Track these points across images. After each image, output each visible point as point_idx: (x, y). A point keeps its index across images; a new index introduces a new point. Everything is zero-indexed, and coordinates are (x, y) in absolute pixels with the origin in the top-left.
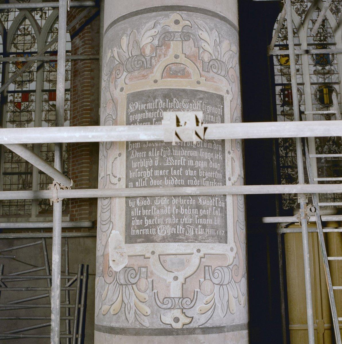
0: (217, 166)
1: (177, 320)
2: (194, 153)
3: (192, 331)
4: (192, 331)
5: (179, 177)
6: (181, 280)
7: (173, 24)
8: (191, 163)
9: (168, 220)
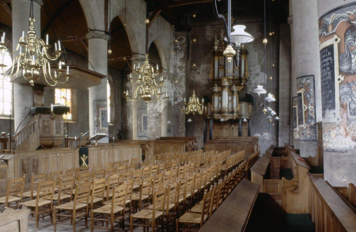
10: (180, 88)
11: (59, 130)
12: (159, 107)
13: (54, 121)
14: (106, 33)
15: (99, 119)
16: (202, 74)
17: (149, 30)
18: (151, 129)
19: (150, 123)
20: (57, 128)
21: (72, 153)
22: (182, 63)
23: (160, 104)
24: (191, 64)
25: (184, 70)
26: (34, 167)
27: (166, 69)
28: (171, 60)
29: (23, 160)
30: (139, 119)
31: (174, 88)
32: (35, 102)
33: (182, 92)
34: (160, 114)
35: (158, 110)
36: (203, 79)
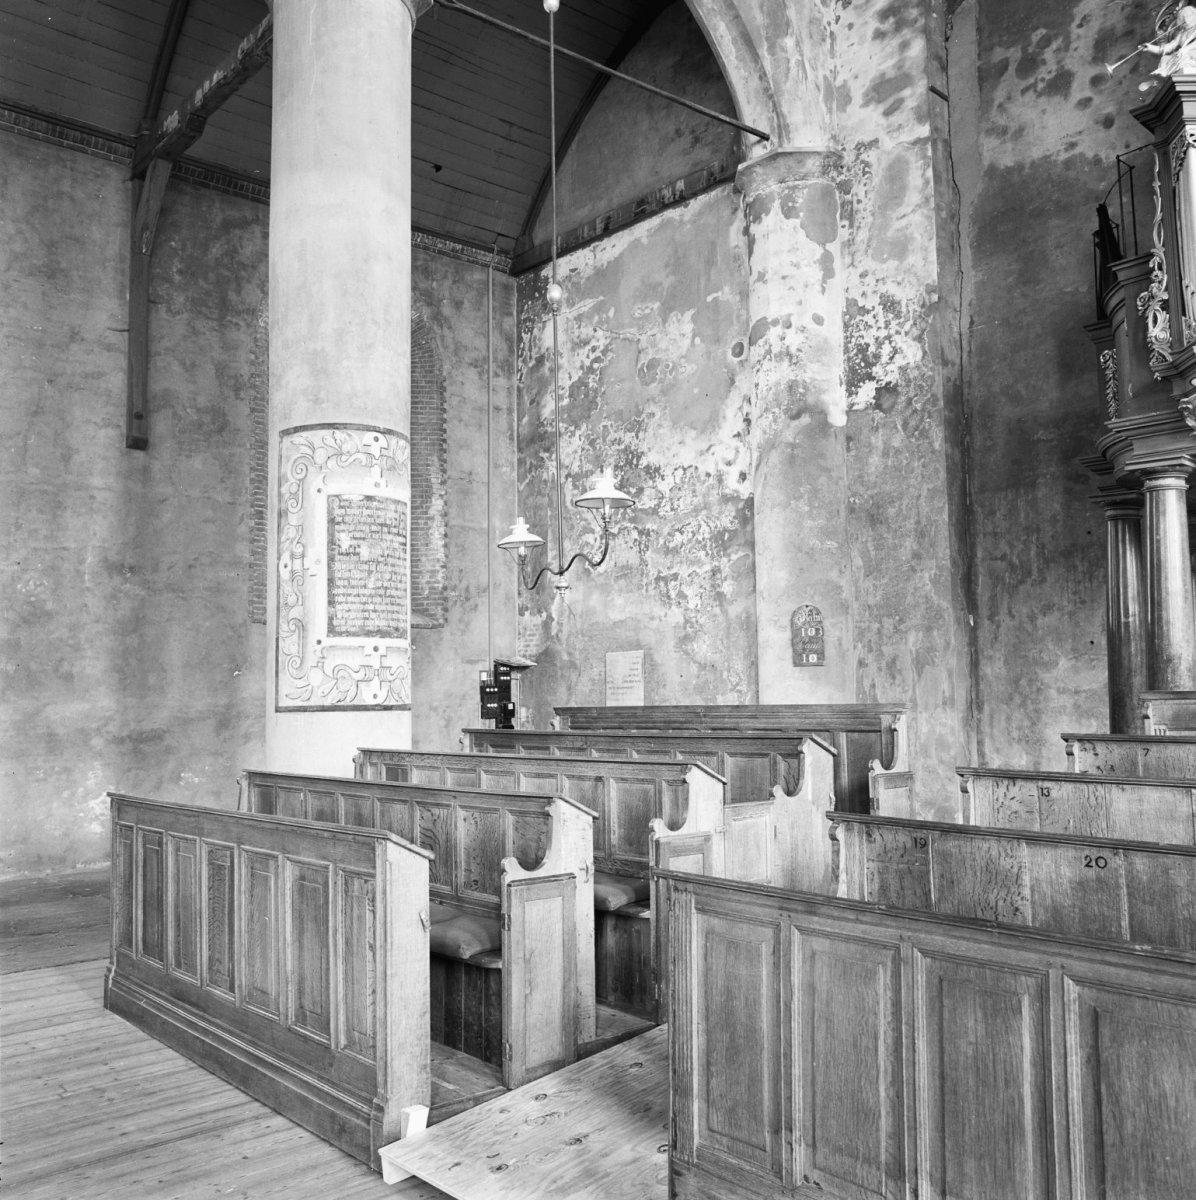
10: (893, 264)
16: (1096, 81)
19: (682, 595)
22: (895, 42)
23: (740, 426)
24: (979, 30)
25: (915, 94)
28: (789, 42)
31: (843, 277)
33: (908, 295)
35: (732, 483)
36: (1108, 122)
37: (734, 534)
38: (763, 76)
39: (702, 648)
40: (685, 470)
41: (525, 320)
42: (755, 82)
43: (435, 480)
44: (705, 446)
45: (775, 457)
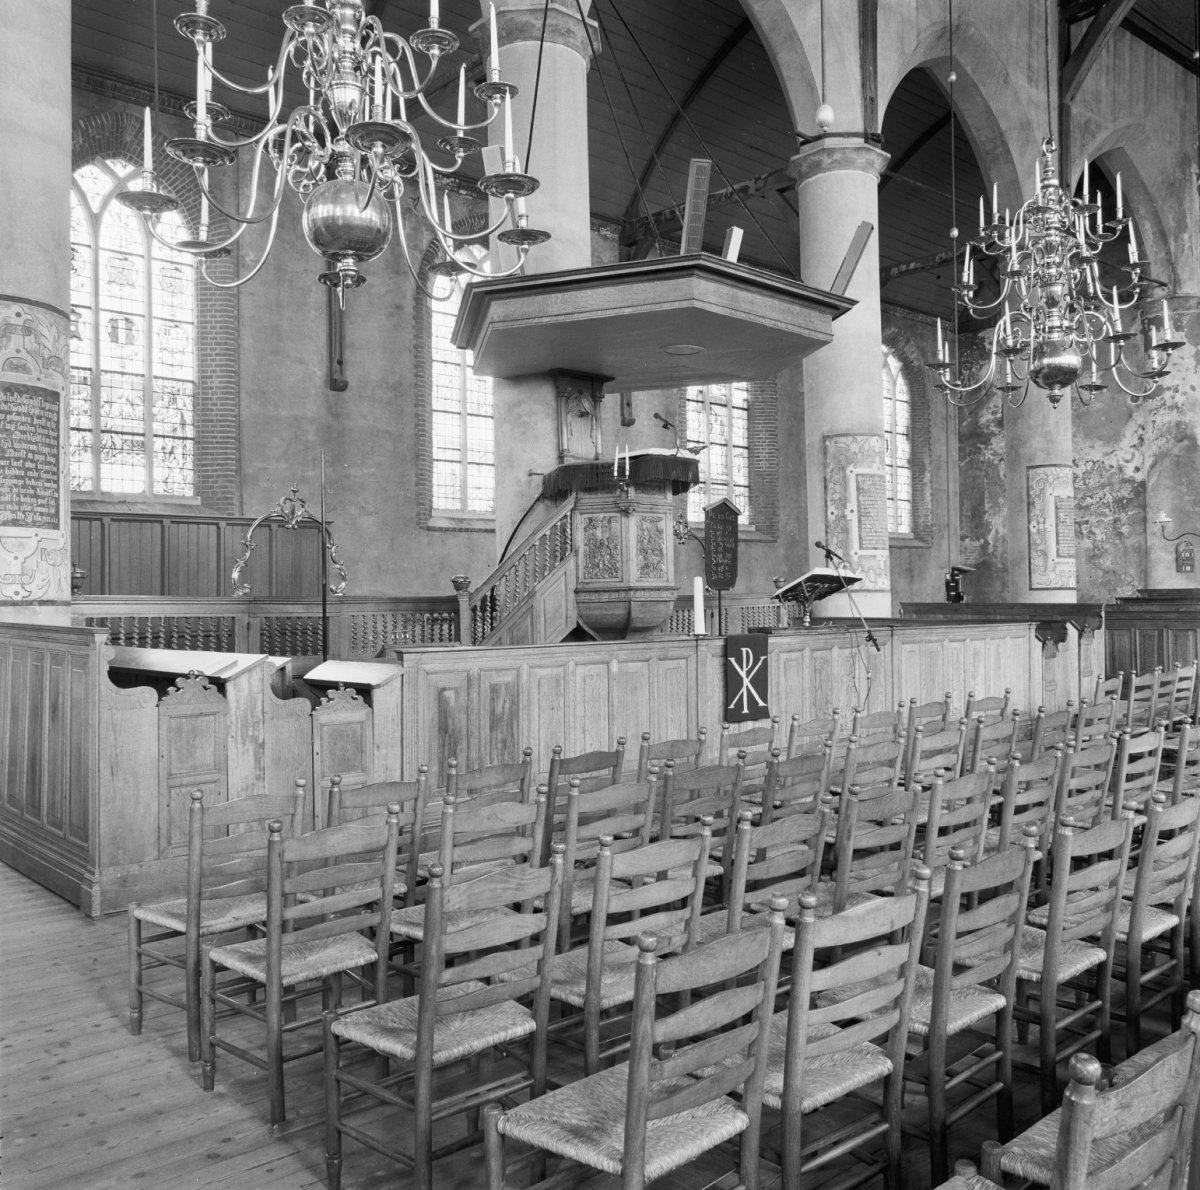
0: (53, 460)
1: (17, 593)
2: (34, 447)
3: (31, 603)
4: (31, 603)
5: (19, 468)
6: (21, 559)
7: (14, 316)
8: (30, 456)
9: (9, 507)
11: (654, 559)
12: (1133, 455)
13: (633, 522)
14: (870, 138)
15: (847, 512)
17: (1075, 110)
18: (1094, 556)
19: (1091, 532)
20: (643, 551)
21: (686, 658)
23: (1136, 441)
26: (495, 723)
27: (1164, 279)
28: (1186, 236)
29: (444, 689)
30: (1036, 511)
32: (565, 447)
34: (1141, 489)
37: (1130, 501)
38: (1168, 252)
39: (1107, 562)
40: (1094, 463)
41: (965, 362)
42: (1162, 255)
43: (927, 462)
44: (1109, 450)
45: (1167, 462)
